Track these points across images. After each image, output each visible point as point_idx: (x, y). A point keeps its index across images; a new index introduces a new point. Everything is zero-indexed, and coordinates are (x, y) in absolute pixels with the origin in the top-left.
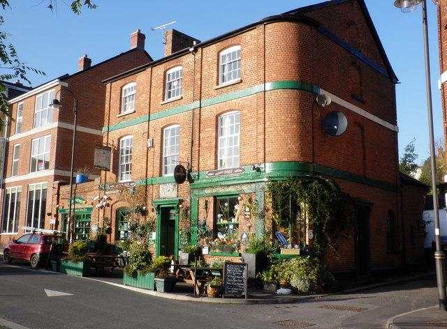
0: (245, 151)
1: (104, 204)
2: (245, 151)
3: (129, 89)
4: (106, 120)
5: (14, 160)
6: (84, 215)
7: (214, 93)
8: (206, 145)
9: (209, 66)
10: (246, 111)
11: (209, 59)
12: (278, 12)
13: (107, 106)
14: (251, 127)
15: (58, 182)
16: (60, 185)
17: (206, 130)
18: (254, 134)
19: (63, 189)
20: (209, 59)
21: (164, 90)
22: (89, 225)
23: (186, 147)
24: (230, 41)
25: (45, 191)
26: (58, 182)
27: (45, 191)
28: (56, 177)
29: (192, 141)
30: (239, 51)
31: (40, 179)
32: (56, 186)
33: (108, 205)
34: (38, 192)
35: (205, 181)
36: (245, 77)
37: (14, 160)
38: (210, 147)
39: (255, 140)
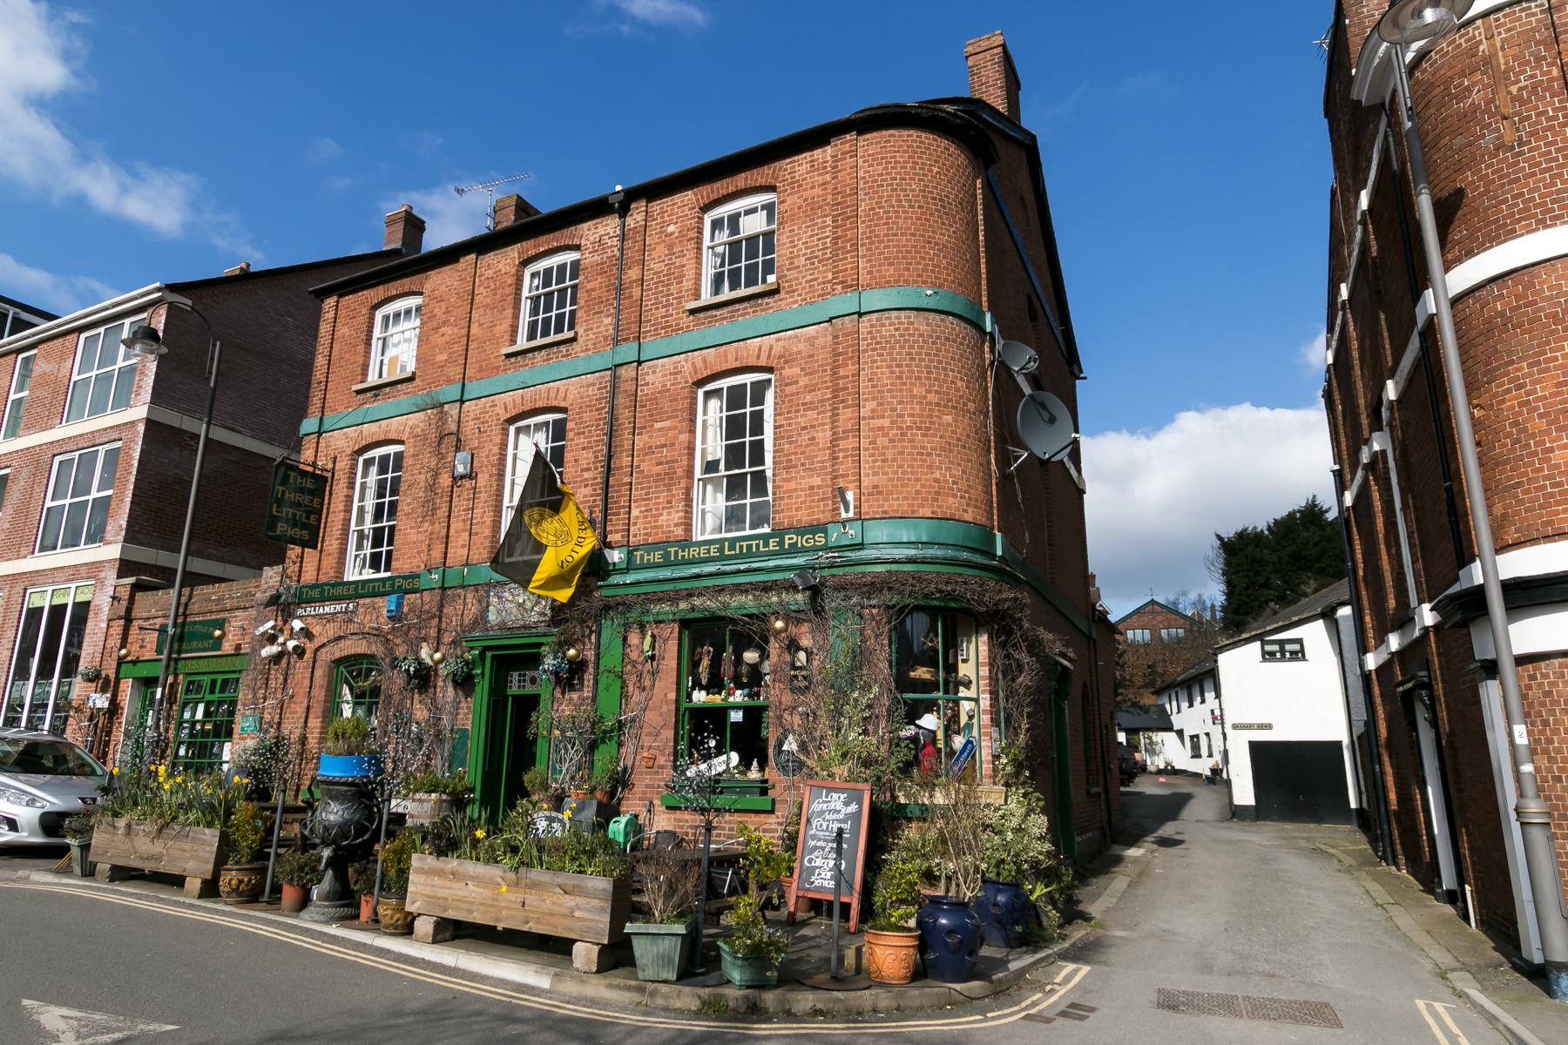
0: (793, 485)
1: (291, 644)
2: (793, 485)
3: (397, 315)
4: (316, 401)
5: (49, 504)
6: (214, 682)
7: (687, 320)
8: (657, 469)
9: (670, 247)
10: (797, 370)
11: (671, 228)
12: (911, 98)
13: (320, 361)
14: (812, 414)
15: (131, 580)
16: (136, 587)
17: (657, 425)
18: (823, 436)
19: (147, 604)
20: (671, 228)
21: (516, 316)
22: (232, 713)
23: (587, 475)
24: (741, 180)
25: (82, 609)
26: (131, 580)
27: (82, 609)
28: (125, 567)
29: (610, 457)
30: (576, 265)
31: (74, 572)
32: (125, 593)
33: (300, 652)
34: (58, 611)
35: (329, 609)
36: (791, 275)
37: (49, 504)
38: (670, 475)
39: (826, 455)
